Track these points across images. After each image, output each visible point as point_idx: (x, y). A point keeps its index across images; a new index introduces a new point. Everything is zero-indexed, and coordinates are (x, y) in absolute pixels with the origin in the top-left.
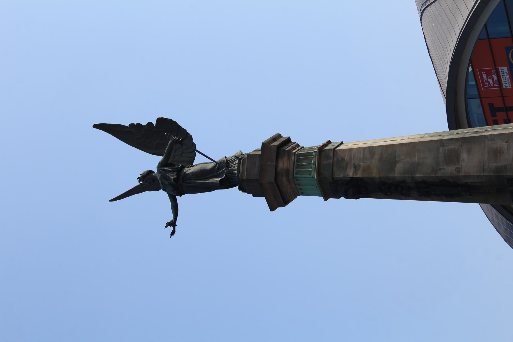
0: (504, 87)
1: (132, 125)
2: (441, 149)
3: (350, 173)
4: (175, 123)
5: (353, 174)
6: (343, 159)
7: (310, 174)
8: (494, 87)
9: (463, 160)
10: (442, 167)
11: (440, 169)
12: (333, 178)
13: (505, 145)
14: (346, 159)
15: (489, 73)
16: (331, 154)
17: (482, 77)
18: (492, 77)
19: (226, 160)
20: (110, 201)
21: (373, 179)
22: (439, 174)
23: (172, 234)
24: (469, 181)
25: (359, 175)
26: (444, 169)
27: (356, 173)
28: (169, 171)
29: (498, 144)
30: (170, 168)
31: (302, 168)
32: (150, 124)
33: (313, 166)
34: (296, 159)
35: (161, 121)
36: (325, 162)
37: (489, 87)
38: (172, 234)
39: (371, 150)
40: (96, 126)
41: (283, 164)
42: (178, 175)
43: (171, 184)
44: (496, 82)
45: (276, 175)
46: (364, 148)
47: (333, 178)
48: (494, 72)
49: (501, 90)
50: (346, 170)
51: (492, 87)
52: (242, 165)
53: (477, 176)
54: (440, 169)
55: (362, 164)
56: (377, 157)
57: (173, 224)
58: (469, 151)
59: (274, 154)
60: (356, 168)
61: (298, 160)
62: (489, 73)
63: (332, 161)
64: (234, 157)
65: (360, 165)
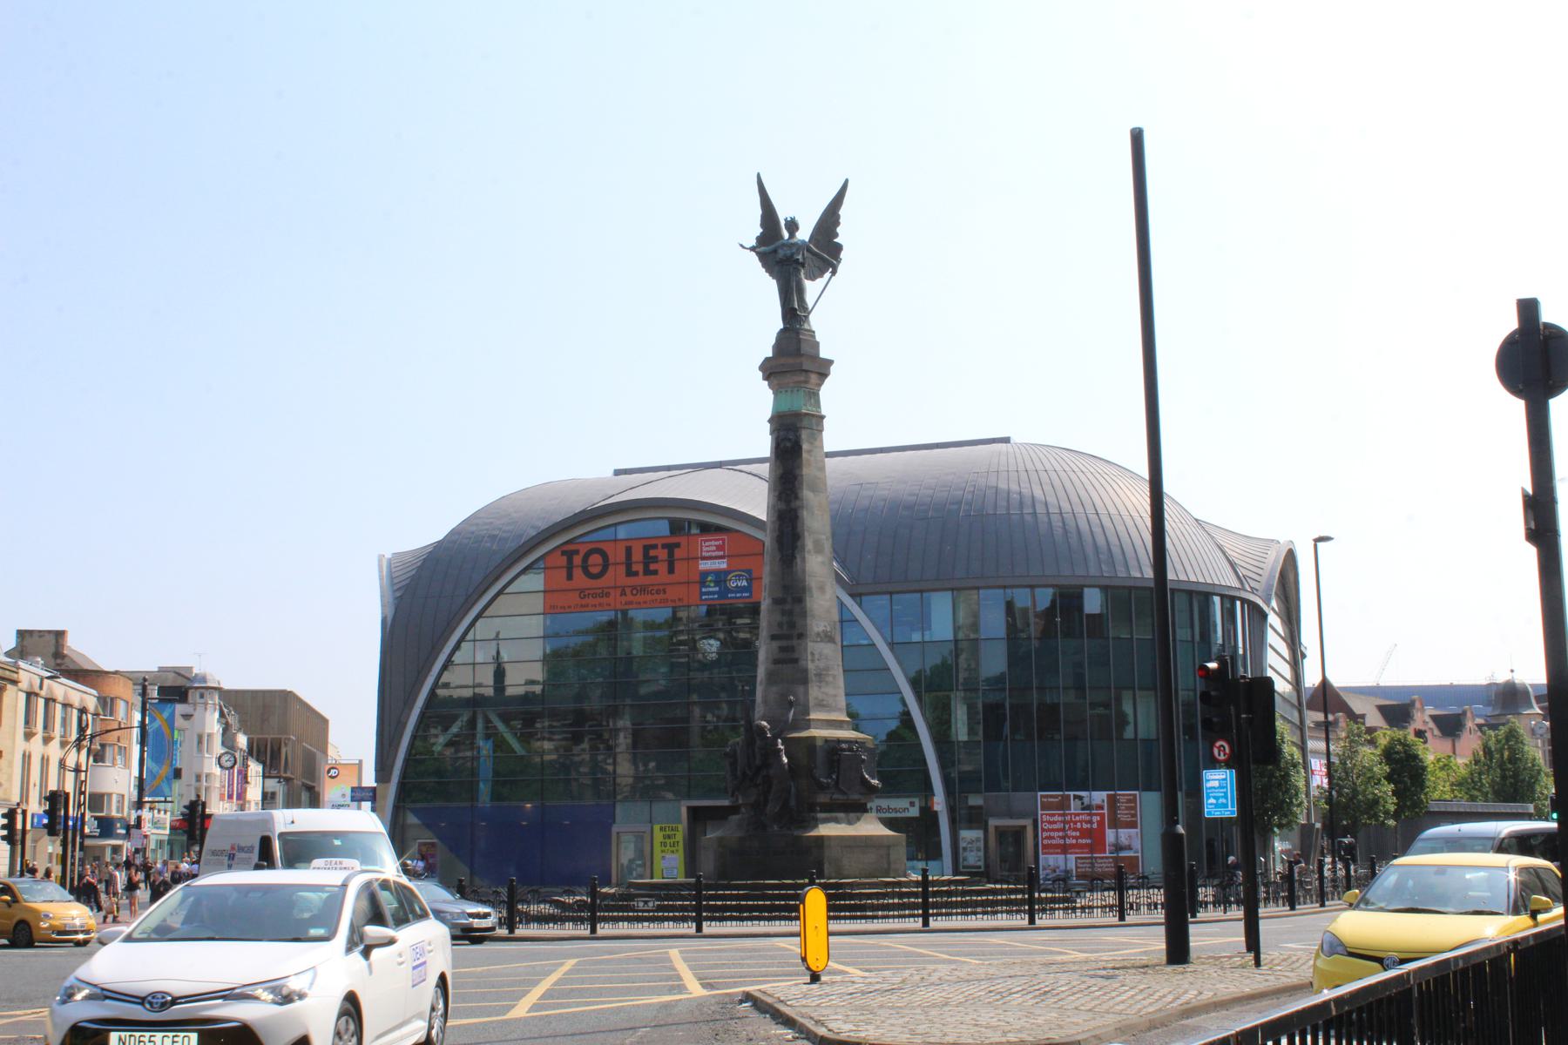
0: (700, 562)
1: (839, 217)
3: (805, 446)
8: (701, 551)
15: (719, 548)
17: (718, 540)
18: (714, 551)
20: (759, 176)
21: (800, 467)
22: (806, 534)
23: (741, 246)
24: (799, 560)
25: (805, 455)
32: (836, 235)
37: (702, 546)
38: (741, 246)
40: (847, 181)
43: (792, 254)
44: (708, 554)
45: (806, 371)
47: (801, 428)
48: (721, 553)
49: (698, 558)
51: (701, 549)
53: (804, 571)
58: (823, 563)
62: (719, 548)
65: (811, 456)
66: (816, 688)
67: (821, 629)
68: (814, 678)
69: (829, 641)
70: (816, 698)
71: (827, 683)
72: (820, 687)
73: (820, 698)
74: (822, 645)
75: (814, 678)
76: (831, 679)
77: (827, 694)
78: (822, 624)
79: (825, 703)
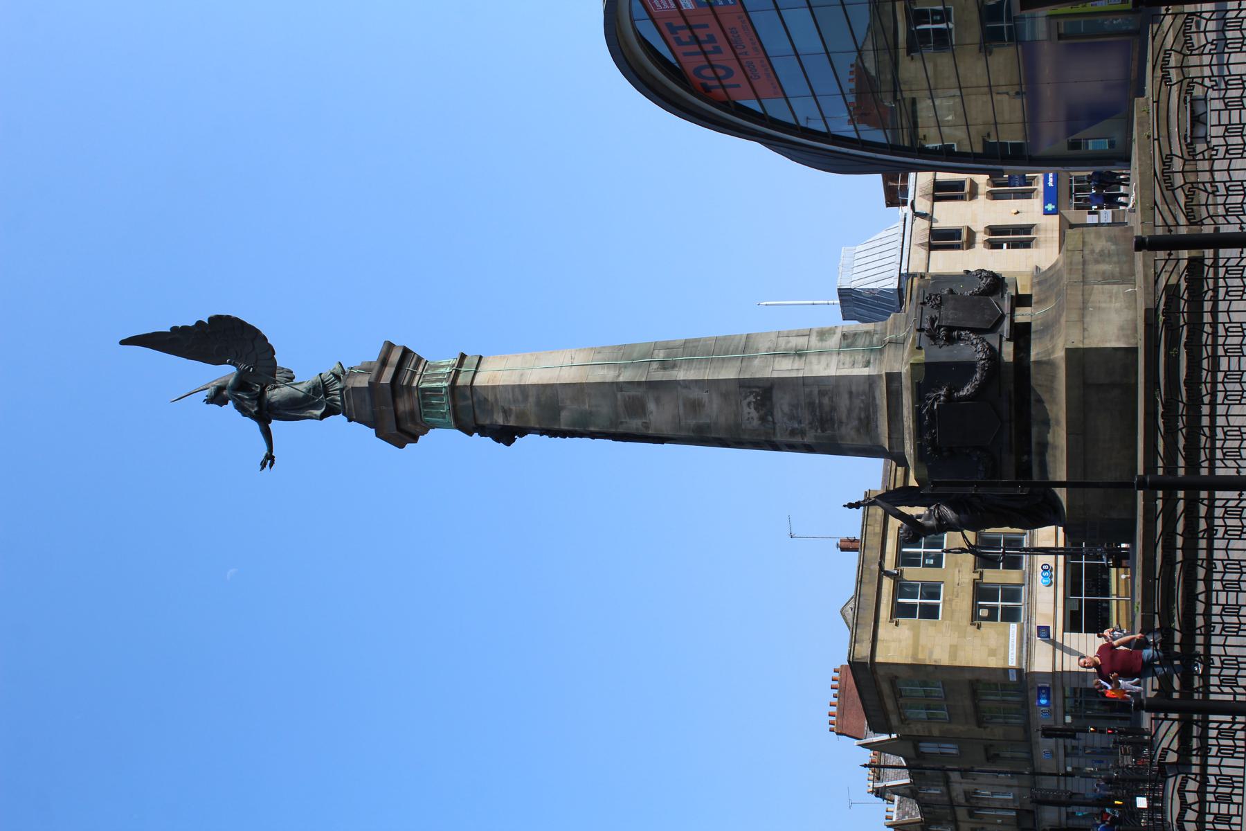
1: (174, 329)
2: (619, 395)
4: (237, 320)
5: (504, 422)
6: (486, 400)
7: (444, 418)
9: (652, 412)
10: (623, 420)
11: (621, 423)
12: (476, 424)
13: (705, 396)
14: (490, 399)
16: (468, 393)
19: (322, 380)
26: (626, 422)
27: (508, 420)
28: (246, 399)
29: (695, 394)
30: (245, 393)
31: (433, 408)
32: (200, 323)
33: (446, 407)
34: (420, 396)
35: (217, 320)
36: (461, 403)
39: (523, 390)
41: (404, 405)
42: (260, 405)
45: (398, 420)
46: (513, 387)
50: (493, 415)
52: (347, 399)
54: (621, 423)
55: (513, 408)
56: (532, 400)
57: (270, 459)
58: (657, 401)
59: (389, 395)
60: (506, 413)
61: (424, 397)
63: (470, 402)
64: (331, 375)
66: (844, 430)
67: (754, 414)
68: (829, 432)
69: (770, 399)
70: (858, 430)
71: (833, 409)
72: (841, 422)
73: (855, 423)
74: (778, 415)
75: (829, 432)
76: (826, 401)
77: (850, 411)
78: (746, 410)
79: (863, 415)
